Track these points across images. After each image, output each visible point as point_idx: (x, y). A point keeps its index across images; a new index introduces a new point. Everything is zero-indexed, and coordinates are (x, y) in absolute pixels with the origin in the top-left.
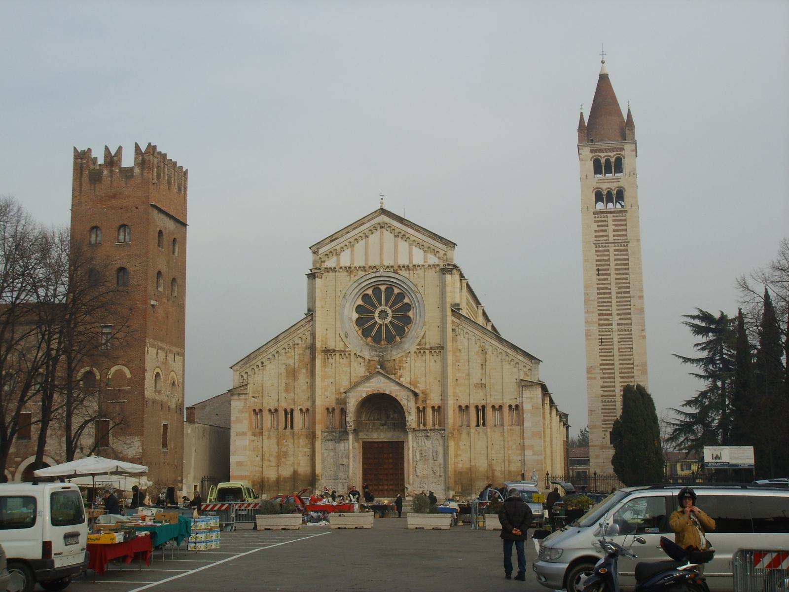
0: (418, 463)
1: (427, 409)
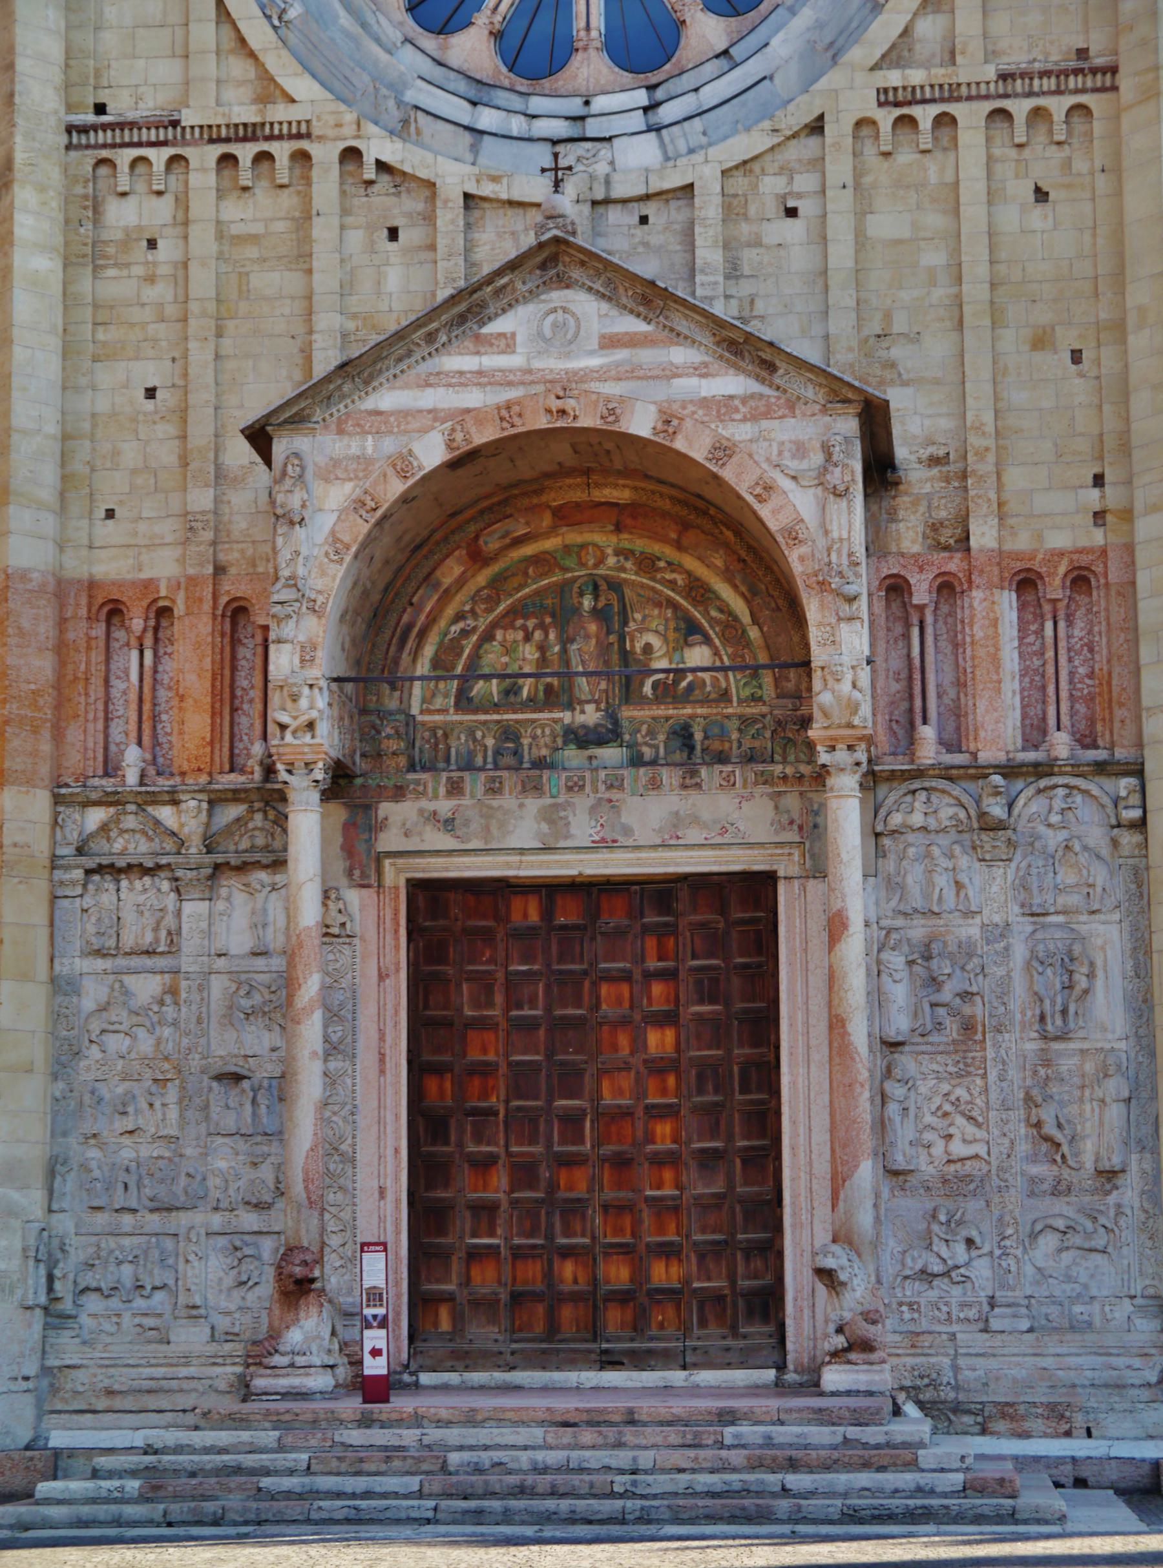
0: (906, 1062)
1: (977, 594)
